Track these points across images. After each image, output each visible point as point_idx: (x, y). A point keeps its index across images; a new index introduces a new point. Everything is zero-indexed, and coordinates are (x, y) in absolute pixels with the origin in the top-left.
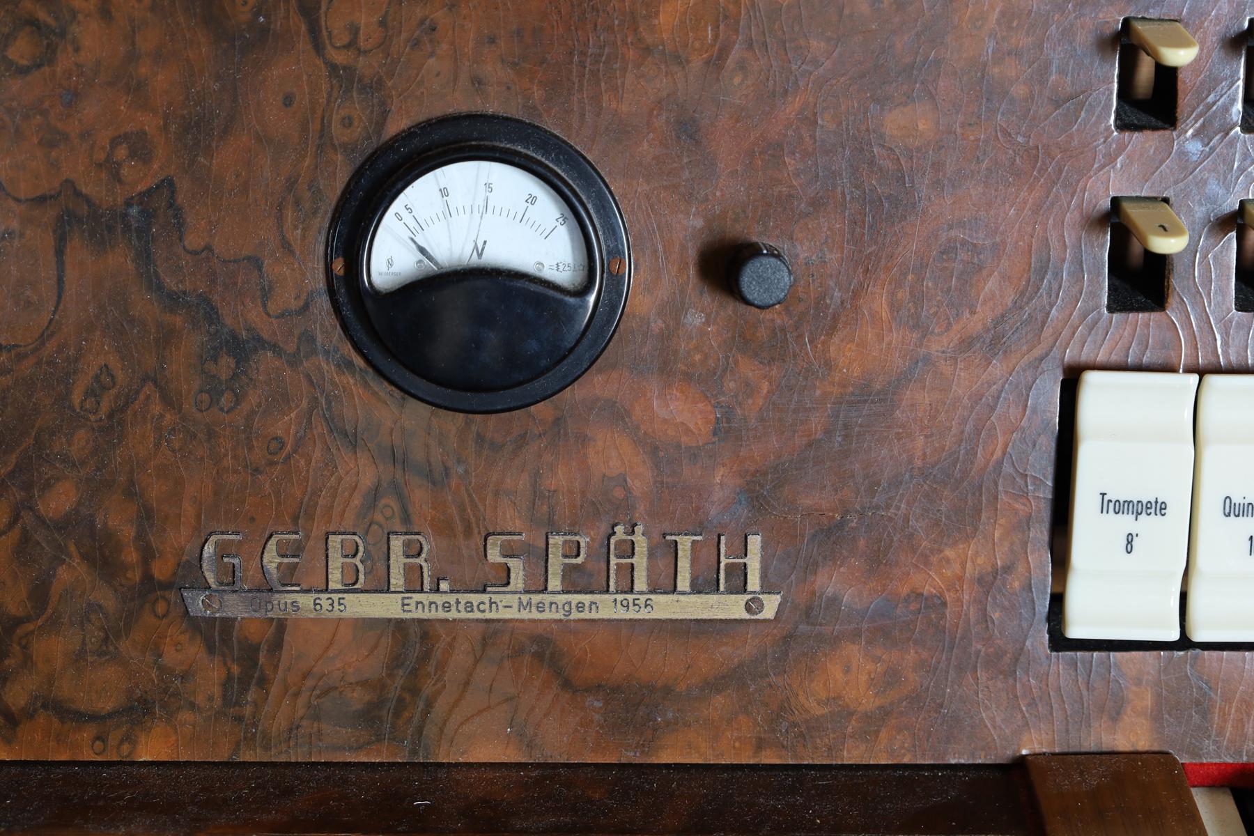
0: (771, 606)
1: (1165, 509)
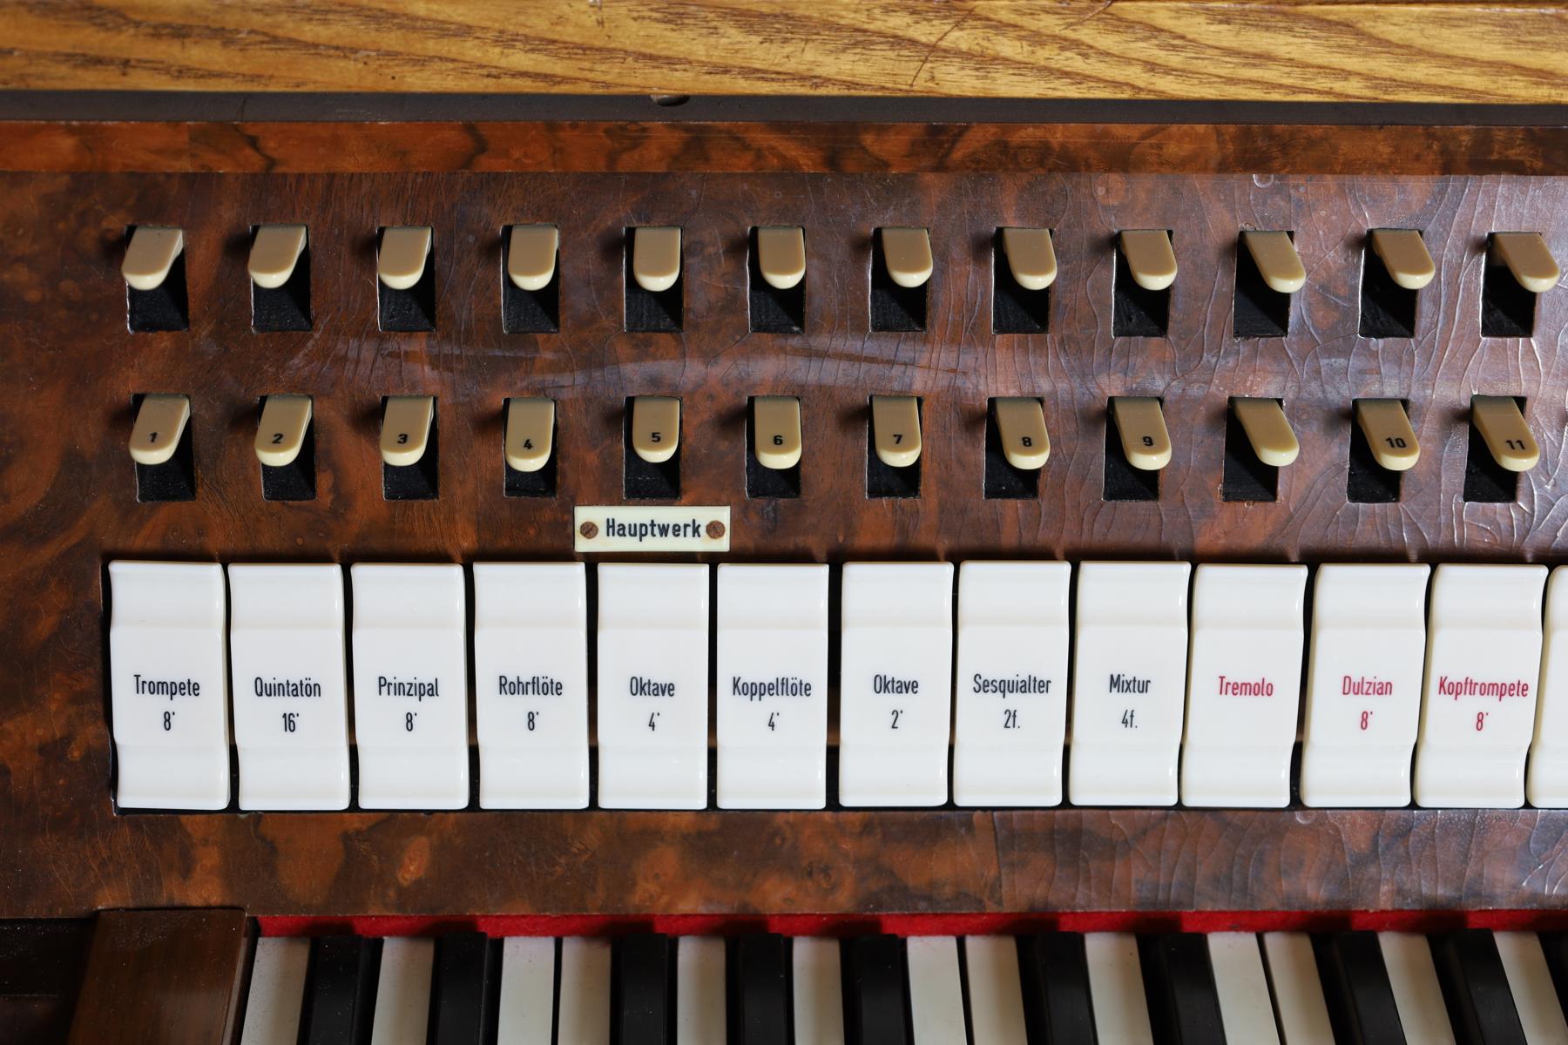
1: (198, 689)
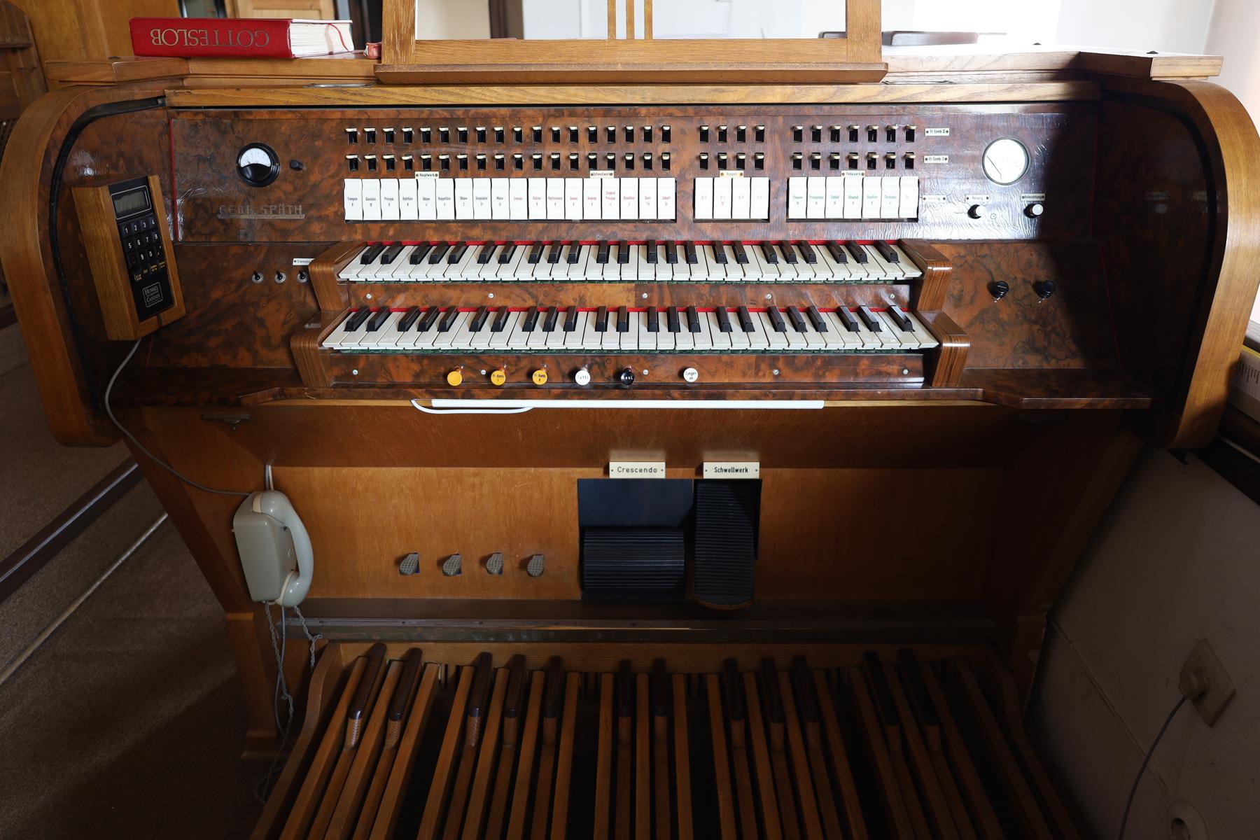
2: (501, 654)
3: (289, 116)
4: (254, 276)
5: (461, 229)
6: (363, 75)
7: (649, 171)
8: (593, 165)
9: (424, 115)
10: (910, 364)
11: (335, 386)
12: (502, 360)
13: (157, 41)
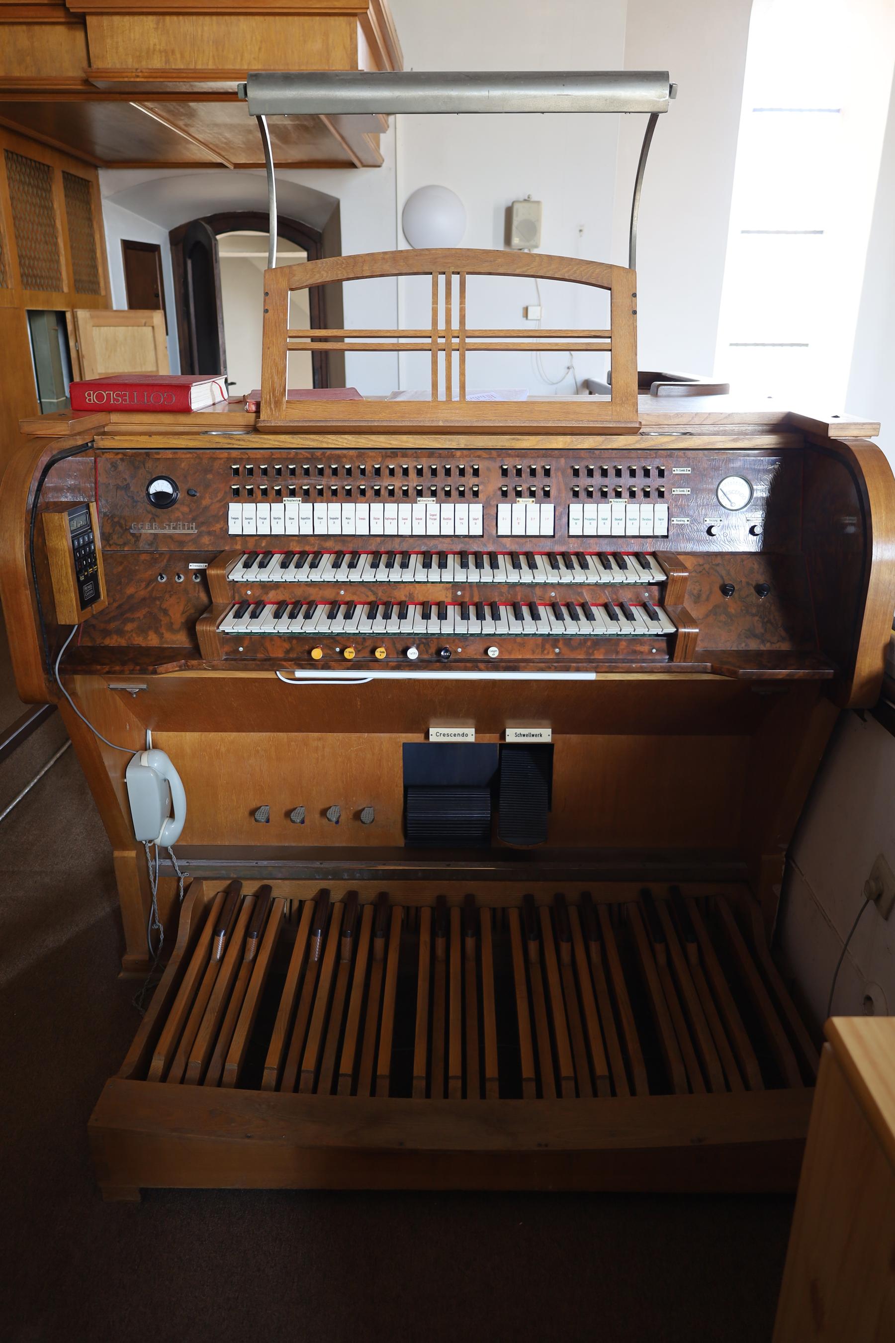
0: (196, 531)
2: (338, 891)
3: (188, 456)
4: (159, 577)
5: (317, 542)
6: (244, 424)
7: (463, 499)
8: (420, 493)
9: (291, 456)
10: (657, 645)
11: (226, 660)
12: (352, 640)
13: (90, 400)
